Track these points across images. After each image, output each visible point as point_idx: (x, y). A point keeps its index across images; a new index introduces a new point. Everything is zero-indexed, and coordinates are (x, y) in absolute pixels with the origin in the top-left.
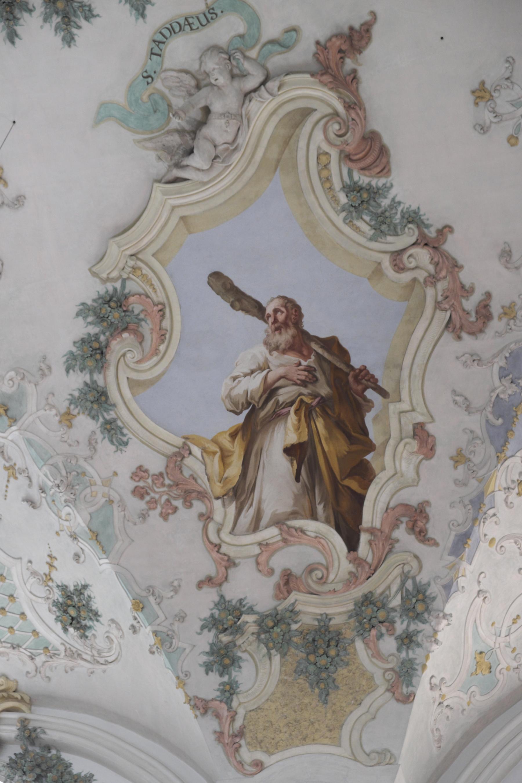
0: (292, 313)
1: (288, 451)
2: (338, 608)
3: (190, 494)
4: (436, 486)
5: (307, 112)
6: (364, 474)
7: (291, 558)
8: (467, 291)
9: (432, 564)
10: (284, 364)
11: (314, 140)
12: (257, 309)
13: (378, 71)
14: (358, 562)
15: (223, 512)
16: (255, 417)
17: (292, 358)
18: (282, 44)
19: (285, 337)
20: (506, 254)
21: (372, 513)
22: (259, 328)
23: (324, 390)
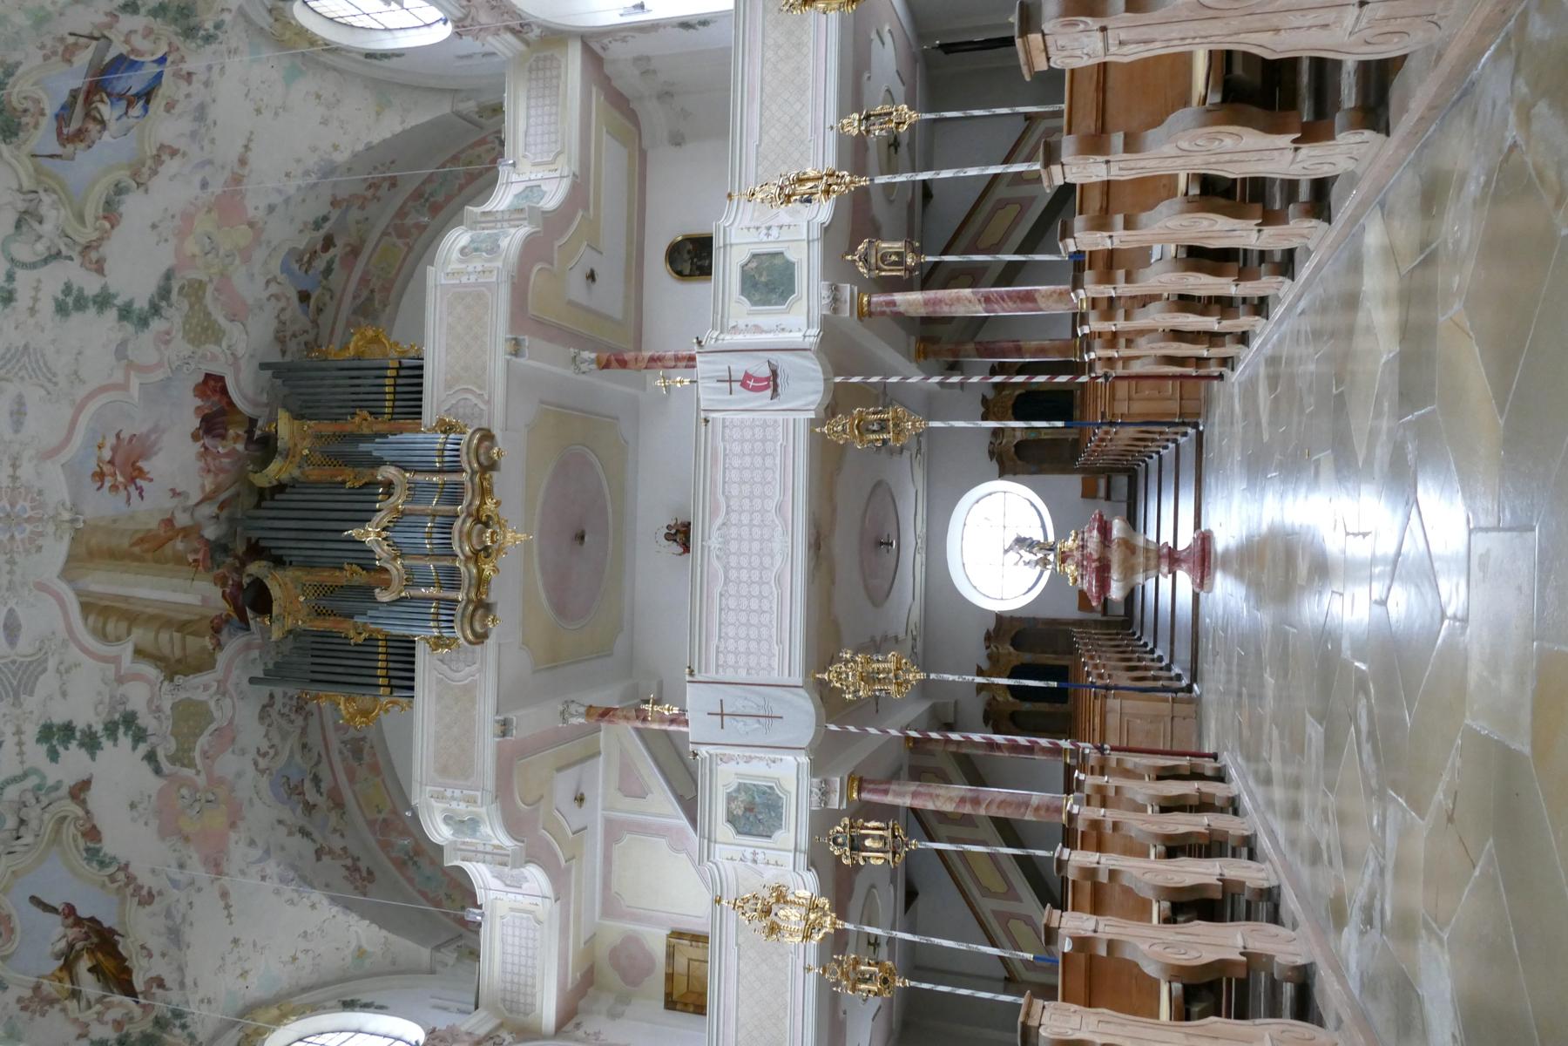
0: (70, 910)
1: (90, 970)
2: (148, 1026)
3: (52, 1002)
4: (159, 967)
5: (65, 818)
6: (128, 971)
7: (115, 1014)
8: (142, 887)
9: (175, 997)
10: (73, 933)
11: (70, 831)
12: (54, 910)
13: (94, 797)
14: (144, 1006)
15: (72, 1005)
16: (68, 962)
17: (76, 930)
18: (56, 787)
19: (70, 920)
20: (153, 871)
21: (139, 984)
22: (58, 919)
23: (95, 940)
